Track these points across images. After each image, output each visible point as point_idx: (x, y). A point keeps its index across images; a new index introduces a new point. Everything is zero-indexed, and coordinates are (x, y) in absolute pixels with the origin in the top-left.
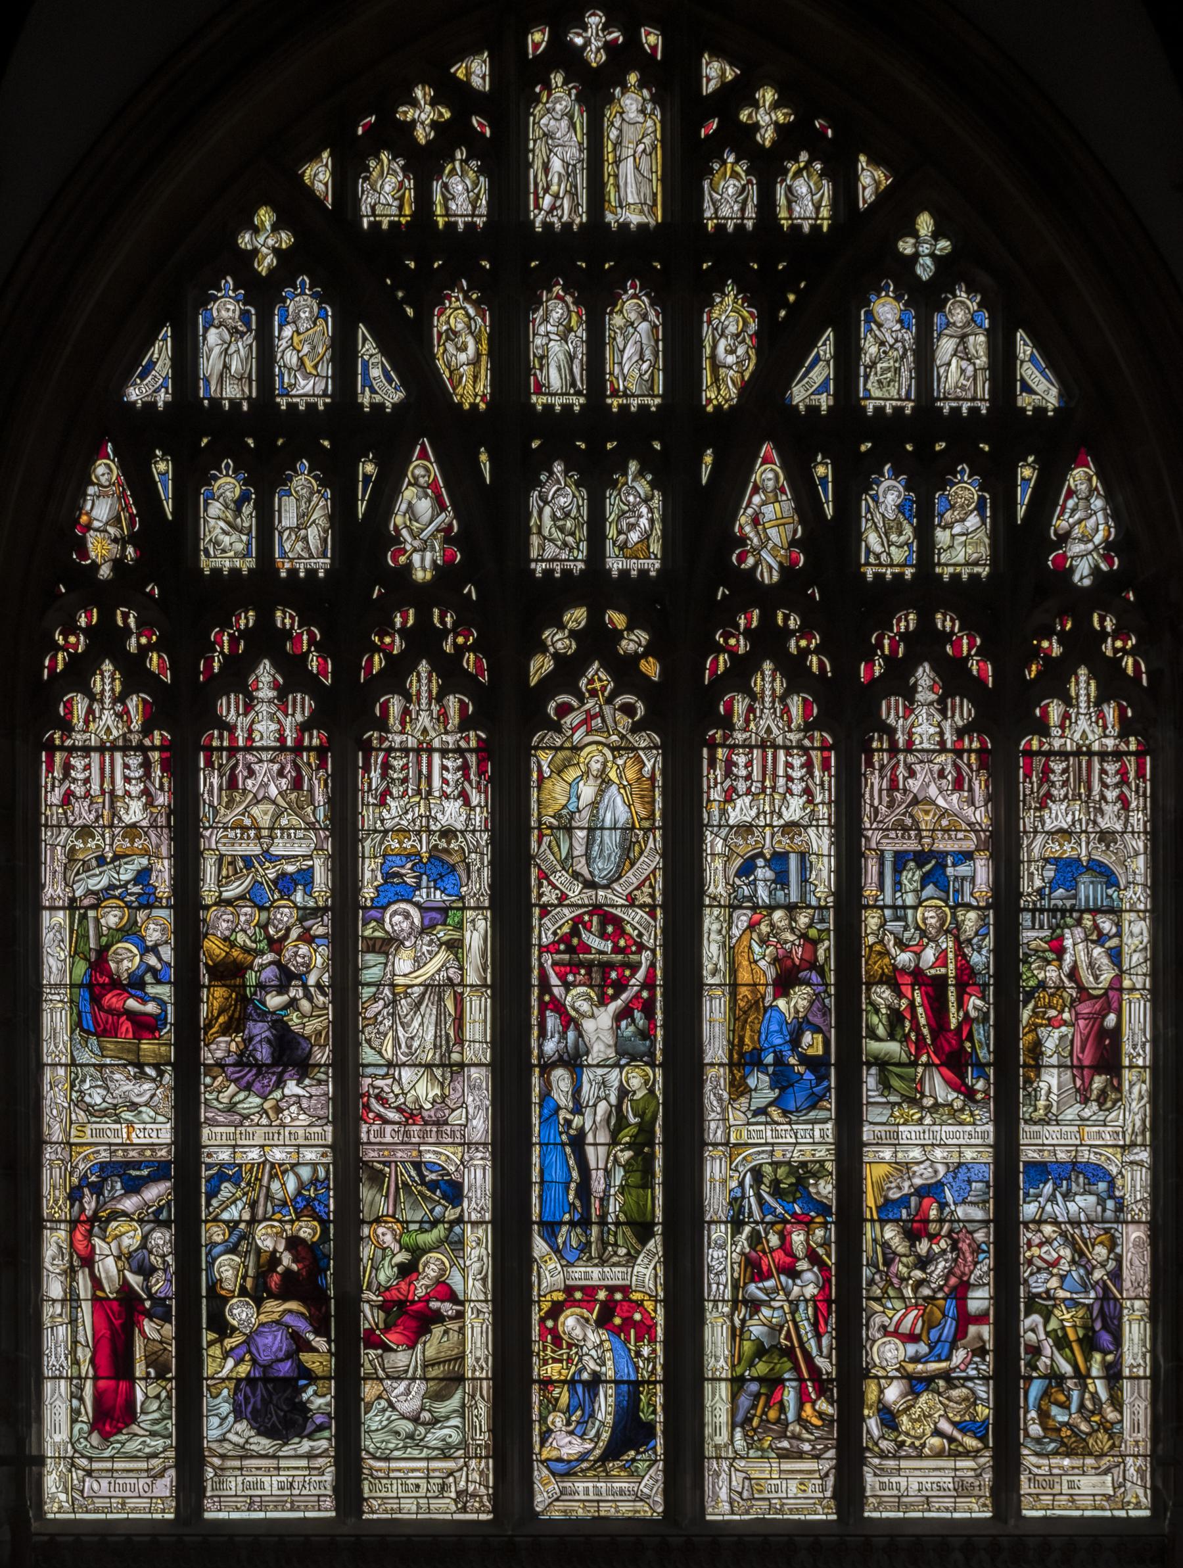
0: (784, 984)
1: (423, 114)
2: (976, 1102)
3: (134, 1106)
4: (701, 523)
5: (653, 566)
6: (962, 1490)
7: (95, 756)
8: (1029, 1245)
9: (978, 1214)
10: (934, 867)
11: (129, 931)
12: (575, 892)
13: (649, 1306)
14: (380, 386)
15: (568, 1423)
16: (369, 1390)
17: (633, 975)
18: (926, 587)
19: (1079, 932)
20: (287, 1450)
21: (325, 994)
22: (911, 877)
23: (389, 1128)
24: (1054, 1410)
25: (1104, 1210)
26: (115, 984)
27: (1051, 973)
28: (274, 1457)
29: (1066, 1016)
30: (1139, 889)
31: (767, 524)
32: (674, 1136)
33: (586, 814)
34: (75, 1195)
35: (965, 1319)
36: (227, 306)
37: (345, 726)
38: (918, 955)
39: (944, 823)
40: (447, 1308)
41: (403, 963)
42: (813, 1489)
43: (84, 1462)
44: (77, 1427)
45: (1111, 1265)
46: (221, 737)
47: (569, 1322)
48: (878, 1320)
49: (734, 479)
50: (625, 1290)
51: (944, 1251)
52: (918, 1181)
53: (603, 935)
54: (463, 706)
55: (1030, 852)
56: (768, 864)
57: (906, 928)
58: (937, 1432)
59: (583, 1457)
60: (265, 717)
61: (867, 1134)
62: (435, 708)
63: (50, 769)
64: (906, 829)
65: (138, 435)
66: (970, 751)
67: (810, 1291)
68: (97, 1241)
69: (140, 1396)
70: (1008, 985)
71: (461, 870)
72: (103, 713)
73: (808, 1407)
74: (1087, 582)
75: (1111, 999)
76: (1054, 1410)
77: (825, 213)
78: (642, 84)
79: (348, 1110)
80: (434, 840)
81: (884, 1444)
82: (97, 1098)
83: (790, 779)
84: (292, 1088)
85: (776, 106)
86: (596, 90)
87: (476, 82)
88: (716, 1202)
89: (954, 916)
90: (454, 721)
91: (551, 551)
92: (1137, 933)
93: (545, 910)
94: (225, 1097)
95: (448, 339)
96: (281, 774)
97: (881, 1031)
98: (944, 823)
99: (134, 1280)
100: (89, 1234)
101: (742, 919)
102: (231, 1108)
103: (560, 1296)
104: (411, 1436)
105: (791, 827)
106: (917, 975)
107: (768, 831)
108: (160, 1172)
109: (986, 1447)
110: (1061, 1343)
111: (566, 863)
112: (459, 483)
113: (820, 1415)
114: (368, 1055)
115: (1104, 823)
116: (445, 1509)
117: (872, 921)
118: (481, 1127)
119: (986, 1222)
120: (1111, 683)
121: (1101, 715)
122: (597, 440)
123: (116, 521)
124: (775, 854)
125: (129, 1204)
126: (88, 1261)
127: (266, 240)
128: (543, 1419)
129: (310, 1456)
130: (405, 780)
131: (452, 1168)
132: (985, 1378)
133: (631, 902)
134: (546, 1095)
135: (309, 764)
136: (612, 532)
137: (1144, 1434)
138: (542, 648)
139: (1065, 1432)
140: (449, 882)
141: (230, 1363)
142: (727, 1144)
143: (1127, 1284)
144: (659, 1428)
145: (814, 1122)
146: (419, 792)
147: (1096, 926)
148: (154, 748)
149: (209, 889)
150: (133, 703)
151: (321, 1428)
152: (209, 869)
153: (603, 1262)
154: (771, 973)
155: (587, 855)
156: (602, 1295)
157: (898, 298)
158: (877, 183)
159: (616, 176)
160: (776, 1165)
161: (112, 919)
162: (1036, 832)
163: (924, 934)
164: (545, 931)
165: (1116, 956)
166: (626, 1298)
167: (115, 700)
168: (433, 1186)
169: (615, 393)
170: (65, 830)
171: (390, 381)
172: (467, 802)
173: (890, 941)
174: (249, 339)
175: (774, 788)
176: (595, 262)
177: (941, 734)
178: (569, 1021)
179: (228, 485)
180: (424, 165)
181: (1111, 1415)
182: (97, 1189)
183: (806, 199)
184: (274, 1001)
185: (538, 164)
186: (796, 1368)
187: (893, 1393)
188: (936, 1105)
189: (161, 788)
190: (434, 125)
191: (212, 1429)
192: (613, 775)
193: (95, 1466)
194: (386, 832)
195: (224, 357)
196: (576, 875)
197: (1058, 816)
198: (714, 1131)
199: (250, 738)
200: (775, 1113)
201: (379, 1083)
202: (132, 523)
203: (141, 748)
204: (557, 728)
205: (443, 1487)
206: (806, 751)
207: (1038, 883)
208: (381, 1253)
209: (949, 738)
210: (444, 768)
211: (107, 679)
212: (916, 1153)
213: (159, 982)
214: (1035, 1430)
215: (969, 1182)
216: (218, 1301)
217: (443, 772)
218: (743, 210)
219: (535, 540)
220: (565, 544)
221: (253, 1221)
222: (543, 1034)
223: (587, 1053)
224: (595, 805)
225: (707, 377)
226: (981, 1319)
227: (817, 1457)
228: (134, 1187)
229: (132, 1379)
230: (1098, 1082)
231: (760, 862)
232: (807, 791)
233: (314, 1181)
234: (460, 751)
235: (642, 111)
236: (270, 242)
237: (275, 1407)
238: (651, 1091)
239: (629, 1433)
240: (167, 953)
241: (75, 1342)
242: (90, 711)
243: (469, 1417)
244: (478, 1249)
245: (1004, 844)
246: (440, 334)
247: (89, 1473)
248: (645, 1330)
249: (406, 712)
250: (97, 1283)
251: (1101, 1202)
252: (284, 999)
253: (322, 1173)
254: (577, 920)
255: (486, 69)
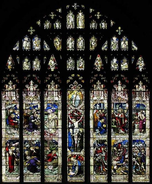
0: (101, 119)
1: (52, 16)
2: (126, 133)
3: (14, 133)
4: (89, 64)
5: (83, 69)
6: (124, 179)
7: (9, 92)
8: (133, 150)
9: (127, 146)
10: (121, 105)
11: (14, 113)
12: (73, 108)
13: (83, 157)
14: (47, 48)
15: (72, 171)
16: (45, 167)
17: (81, 118)
18: (120, 71)
19: (140, 113)
20: (34, 174)
21: (39, 120)
22: (118, 106)
23: (48, 136)
24: (137, 169)
25: (143, 145)
26: (12, 119)
27: (136, 117)
28: (33, 175)
29: (138, 122)
30: (148, 107)
31: (98, 63)
32: (86, 136)
33: (74, 99)
34: (6, 144)
35: (125, 158)
36: (26, 39)
37: (42, 90)
38: (119, 115)
39: (122, 99)
40: (56, 157)
41: (50, 116)
42: (104, 179)
43: (7, 175)
44: (7, 171)
45: (144, 152)
46: (26, 90)
47: (72, 159)
48: (113, 159)
49: (94, 59)
50: (80, 155)
51: (122, 150)
52: (118, 142)
53: (76, 113)
54: (58, 86)
55: (134, 103)
56: (99, 104)
57: (117, 112)
58: (121, 172)
59: (74, 175)
60: (32, 87)
61: (112, 137)
62: (54, 86)
63: (3, 94)
64: (117, 100)
65: (14, 54)
66: (125, 91)
67: (104, 155)
68: (9, 149)
69: (15, 168)
70: (131, 118)
71: (58, 105)
72: (10, 87)
73: (104, 169)
74: (141, 71)
75: (144, 120)
76: (137, 169)
77: (106, 27)
78: (81, 12)
79: (43, 134)
80: (54, 102)
81: (114, 173)
82: (9, 132)
83: (101, 94)
84: (35, 131)
85: (99, 14)
86: (76, 14)
87: (60, 11)
88: (92, 144)
89: (123, 111)
90: (57, 88)
91: (69, 67)
92: (148, 112)
93: (69, 110)
94: (26, 132)
95: (56, 42)
96: (34, 94)
97: (114, 124)
98: (122, 99)
99: (14, 154)
100: (8, 149)
101: (95, 111)
102: (27, 133)
103: (71, 156)
104: (51, 172)
105: (102, 100)
106: (118, 118)
107: (99, 101)
108: (17, 141)
109: (128, 174)
110: (138, 161)
111: (72, 104)
112: (57, 60)
113: (105, 170)
114: (45, 127)
115: (143, 100)
116: (56, 181)
117: (112, 111)
118: (60, 136)
119: (127, 147)
120: (144, 83)
121: (143, 87)
122: (76, 54)
123: (11, 64)
124: (99, 103)
125: (13, 145)
126: (8, 152)
127: (31, 31)
128: (69, 170)
129: (37, 175)
130: (50, 95)
131: (56, 141)
132: (127, 166)
133: (80, 109)
134: (69, 131)
135: (37, 93)
136: (78, 65)
137: (149, 172)
138: (69, 79)
139: (138, 172)
140: (56, 107)
141: (27, 164)
142: (93, 138)
143: (146, 154)
144: (84, 171)
145: (104, 135)
146: (52, 96)
147: (142, 112)
148: (17, 91)
149: (24, 107)
150: (14, 86)
151: (39, 171)
152: (24, 105)
153: (76, 152)
154: (99, 117)
155: (74, 103)
156: (76, 156)
157: (116, 37)
158: (113, 23)
159: (78, 23)
160: (100, 140)
161: (11, 111)
162: (134, 100)
163: (119, 113)
164: (69, 113)
165: (145, 115)
166: (80, 156)
167: (11, 85)
168: (54, 143)
169: (78, 49)
170: (5, 101)
171: (48, 47)
172: (58, 97)
173: (115, 114)
174: (29, 42)
175: (99, 95)
176: (75, 33)
177: (122, 89)
178: (72, 123)
179: (27, 60)
180: (53, 22)
181: (144, 170)
182: (9, 143)
183: (104, 25)
184: (33, 121)
185: (68, 21)
186: (102, 164)
187: (115, 167)
188: (121, 133)
189: (18, 96)
190: (54, 17)
191: (25, 171)
192: (78, 94)
193: (9, 176)
194: (48, 101)
195: (26, 44)
196: (73, 106)
197: (137, 99)
198: (91, 136)
199: (29, 90)
200: (99, 134)
201: (47, 130)
202: (14, 64)
203: (15, 91)
204: (71, 88)
205: (55, 178)
206: (103, 91)
207: (135, 107)
208: (47, 150)
209: (123, 89)
210: (55, 93)
211: (10, 83)
212: (118, 139)
213: (17, 119)
214: (134, 172)
215: (125, 142)
216: (25, 156)
217: (55, 94)
218: (95, 27)
219: (67, 66)
220: (72, 67)
221: (30, 147)
222: (69, 125)
223: (75, 127)
224: (75, 97)
225: (90, 46)
226: (127, 158)
227: (105, 175)
228: (14, 143)
229: (14, 166)
230: (143, 130)
231: (98, 104)
232: (104, 96)
233: (38, 142)
234: (57, 91)
235: (82, 15)
236: (32, 31)
237: (33, 169)
238: (83, 131)
239: (80, 172)
240: (19, 115)
241: (6, 161)
242: (8, 87)
243: (59, 170)
244: (60, 150)
245: (130, 102)
246: (55, 42)
247: (8, 177)
248: (82, 160)
249: (50, 86)
250: (9, 154)
251: (143, 145)
252: (34, 120)
253: (39, 141)
254: (73, 112)
255: (61, 10)
